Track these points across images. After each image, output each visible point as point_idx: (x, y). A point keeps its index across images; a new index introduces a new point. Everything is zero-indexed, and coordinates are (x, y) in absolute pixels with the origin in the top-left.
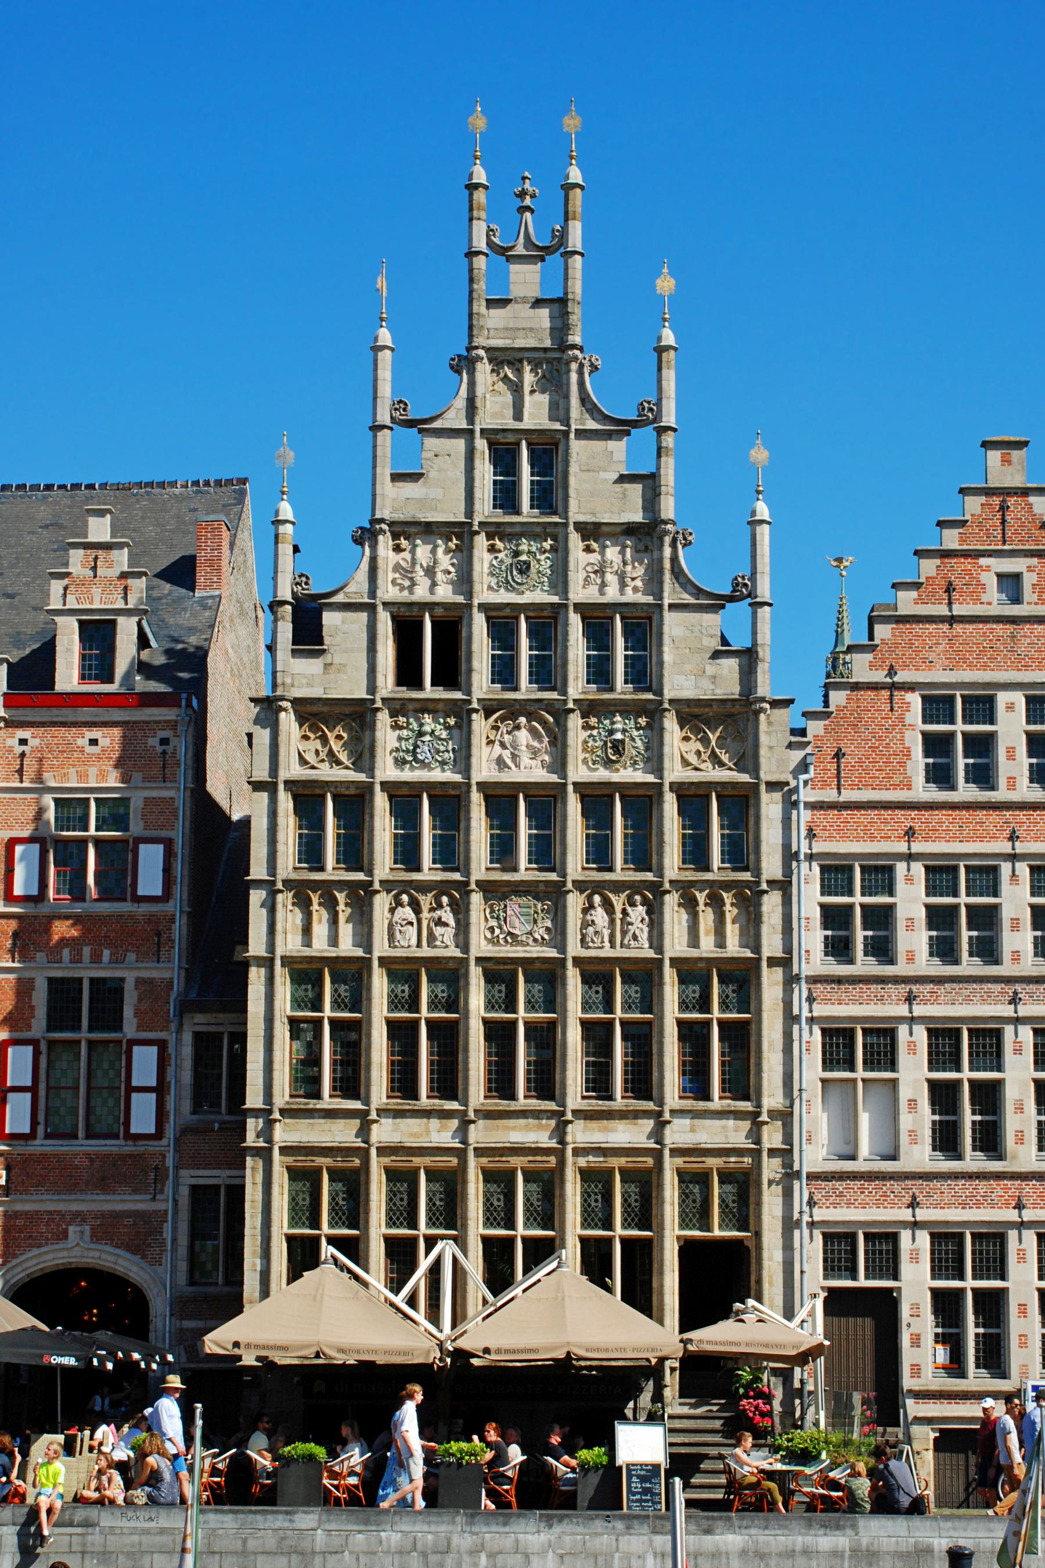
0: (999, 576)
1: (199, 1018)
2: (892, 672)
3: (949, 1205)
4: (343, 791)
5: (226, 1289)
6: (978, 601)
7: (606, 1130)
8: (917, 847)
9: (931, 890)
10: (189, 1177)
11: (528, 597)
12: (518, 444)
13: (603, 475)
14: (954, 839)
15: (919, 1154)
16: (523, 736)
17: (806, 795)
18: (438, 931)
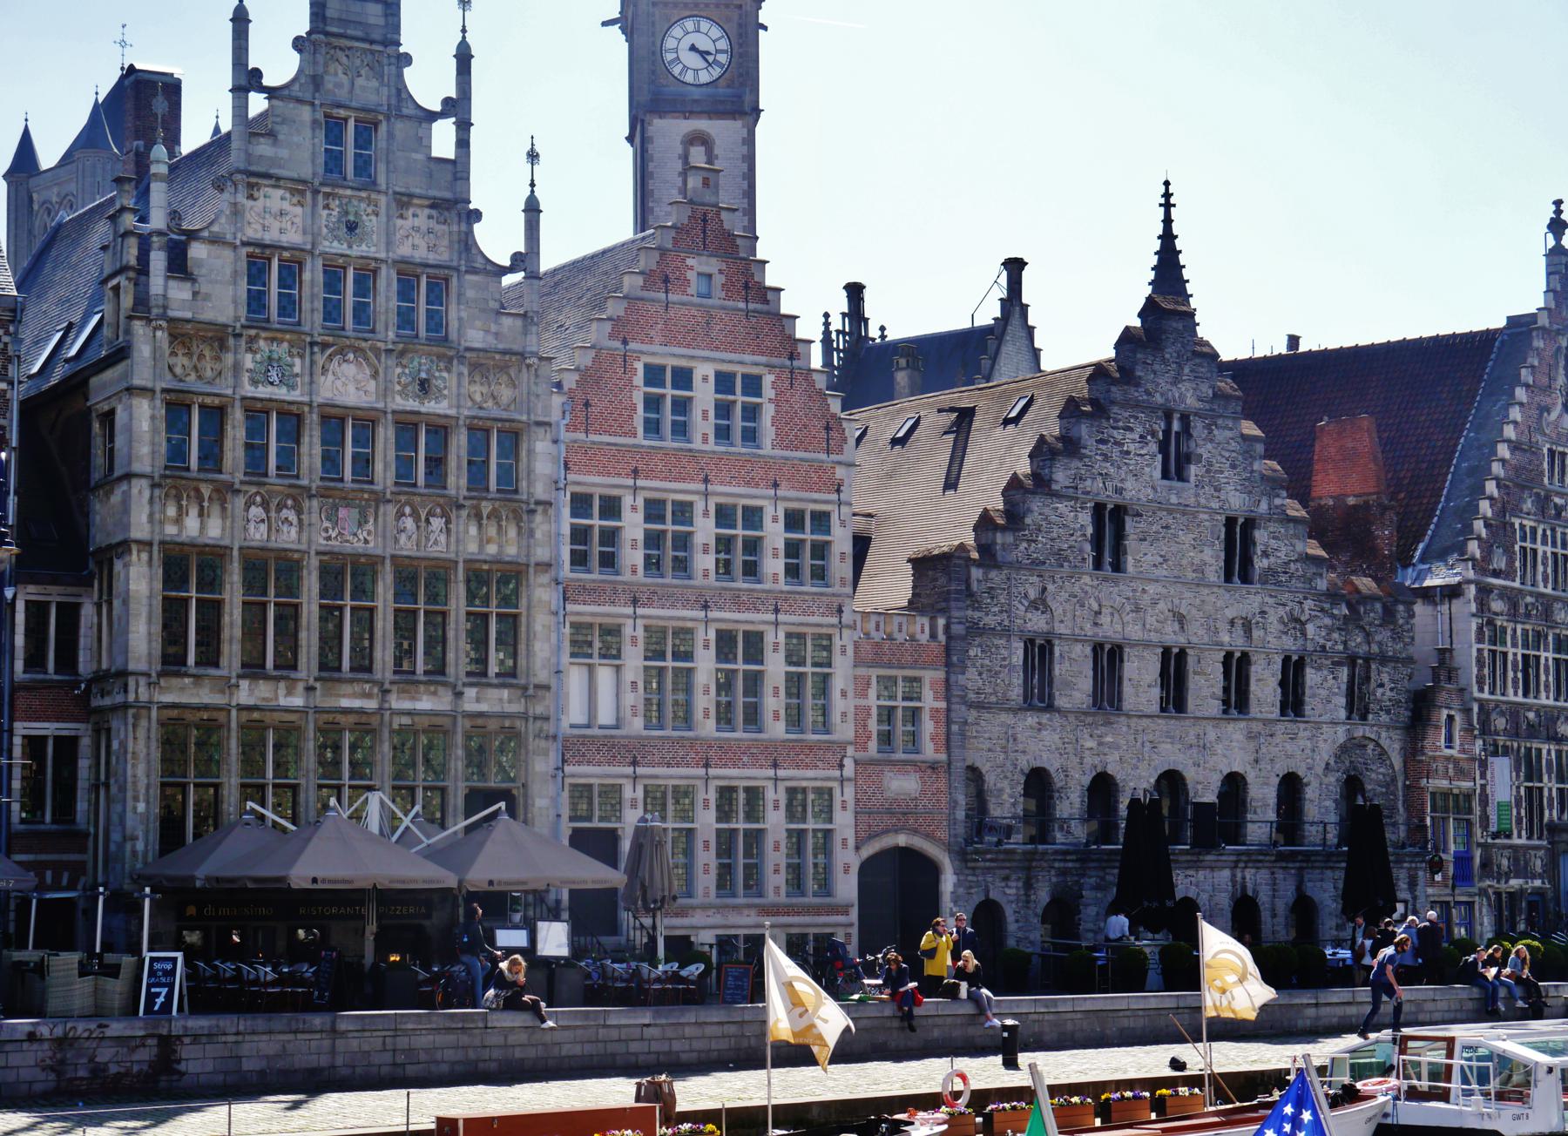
0: (699, 274)
1: (31, 588)
2: (625, 342)
3: (659, 764)
4: (208, 400)
5: (55, 827)
6: (684, 292)
7: (413, 699)
8: (640, 483)
9: (648, 518)
10: (22, 728)
11: (356, 251)
12: (346, 120)
13: (415, 156)
14: (665, 479)
15: (637, 725)
16: (350, 370)
17: (565, 436)
18: (285, 528)
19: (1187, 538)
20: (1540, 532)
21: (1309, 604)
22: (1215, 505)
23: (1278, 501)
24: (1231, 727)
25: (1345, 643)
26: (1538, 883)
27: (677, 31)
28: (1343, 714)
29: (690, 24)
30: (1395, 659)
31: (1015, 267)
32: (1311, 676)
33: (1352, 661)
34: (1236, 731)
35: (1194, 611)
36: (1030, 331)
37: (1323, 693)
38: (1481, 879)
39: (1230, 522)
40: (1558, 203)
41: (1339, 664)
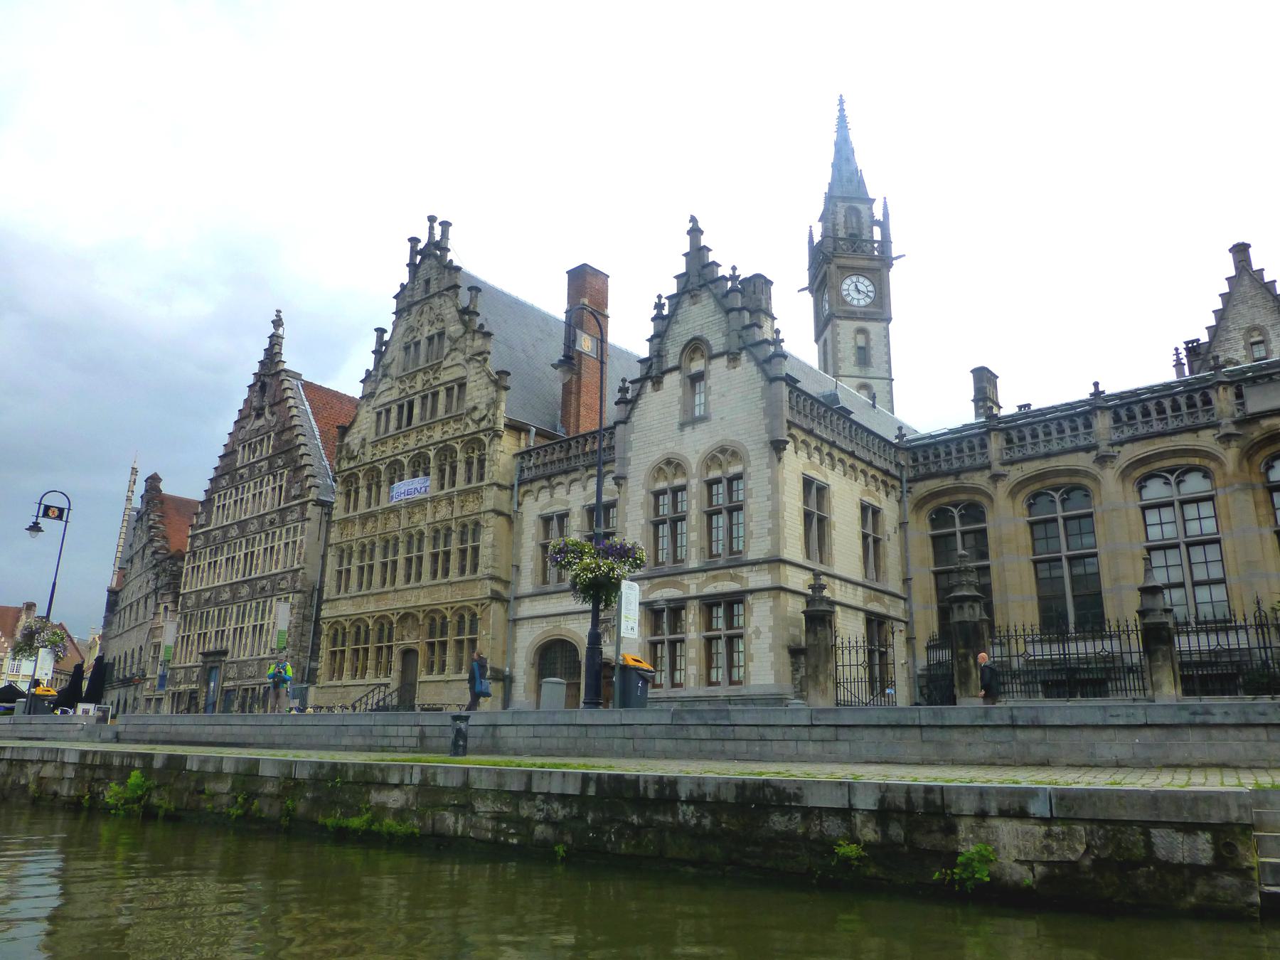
26: (194, 686)
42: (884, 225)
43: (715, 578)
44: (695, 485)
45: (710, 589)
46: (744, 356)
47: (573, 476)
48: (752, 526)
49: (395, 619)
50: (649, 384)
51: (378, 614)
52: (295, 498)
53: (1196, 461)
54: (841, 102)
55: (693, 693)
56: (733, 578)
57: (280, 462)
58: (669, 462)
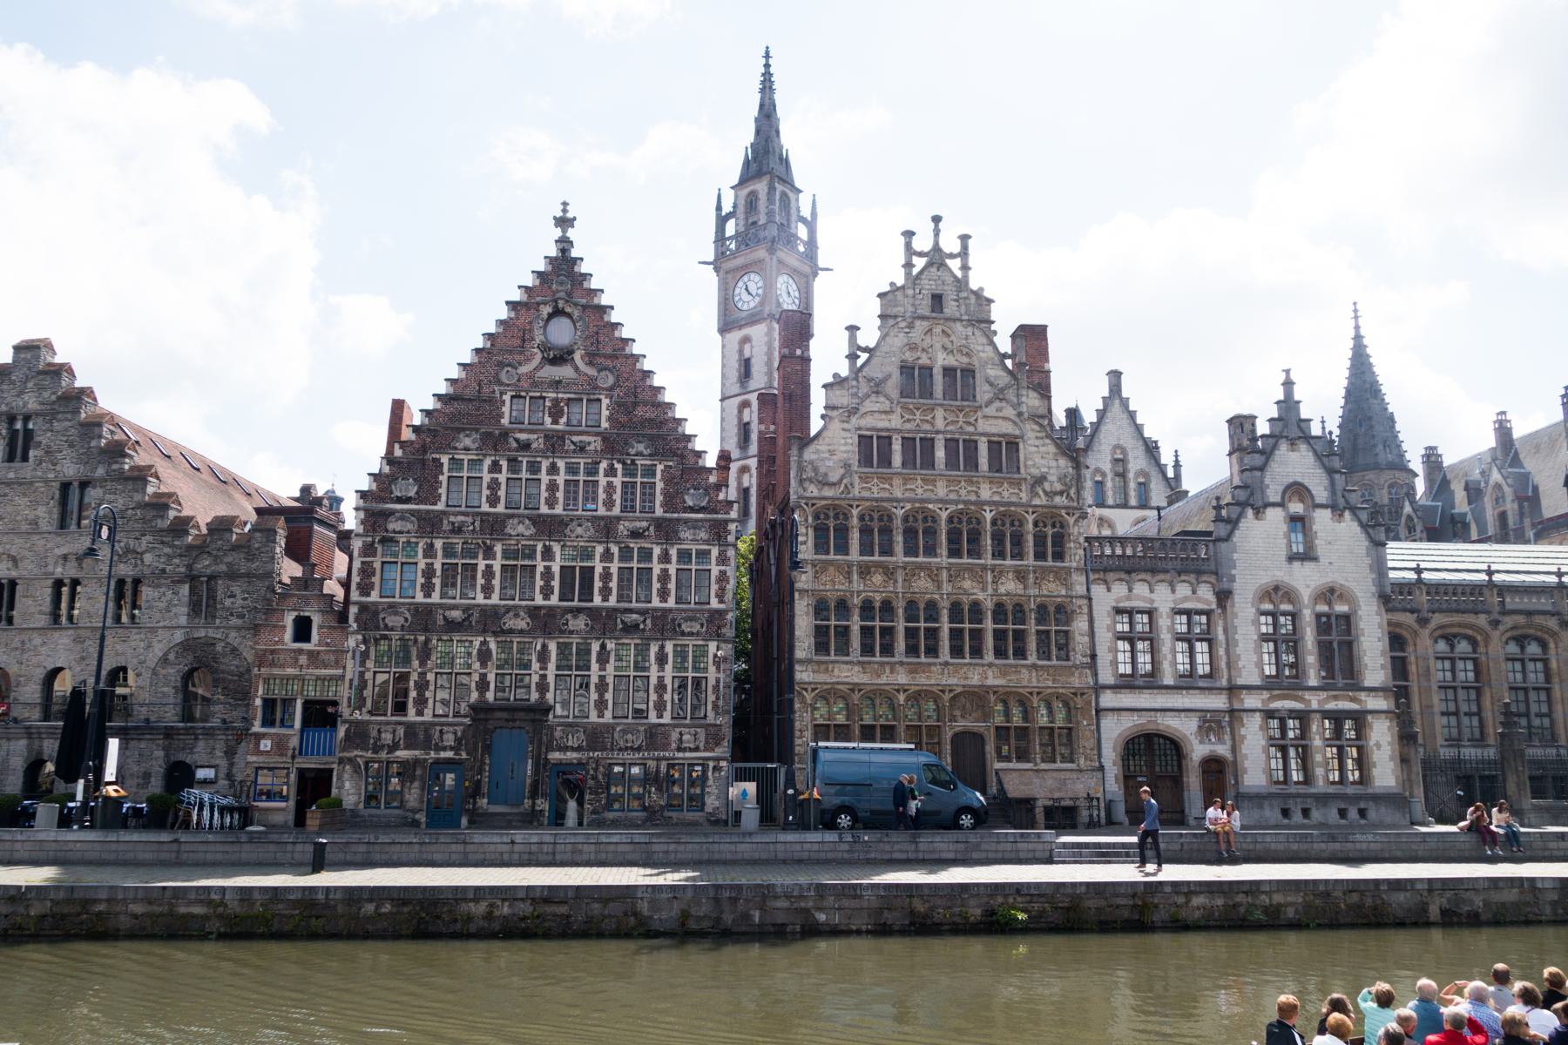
19: (22, 501)
20: (488, 462)
21: (144, 540)
22: (51, 476)
23: (115, 467)
24: (57, 634)
25: (189, 567)
27: (740, 284)
28: (183, 620)
29: (745, 278)
30: (248, 575)
31: (1115, 376)
32: (146, 592)
33: (192, 578)
34: (63, 639)
35: (26, 553)
36: (1132, 416)
37: (162, 605)
38: (343, 750)
39: (65, 487)
40: (565, 204)
41: (181, 582)
42: (811, 226)
43: (1336, 698)
44: (1307, 615)
45: (1331, 706)
46: (1347, 514)
47: (1162, 576)
48: (1366, 660)
49: (947, 697)
50: (1250, 512)
51: (914, 688)
52: (692, 510)
53: (1470, 632)
54: (767, 56)
55: (1323, 791)
56: (1353, 700)
57: (641, 447)
58: (1276, 588)
